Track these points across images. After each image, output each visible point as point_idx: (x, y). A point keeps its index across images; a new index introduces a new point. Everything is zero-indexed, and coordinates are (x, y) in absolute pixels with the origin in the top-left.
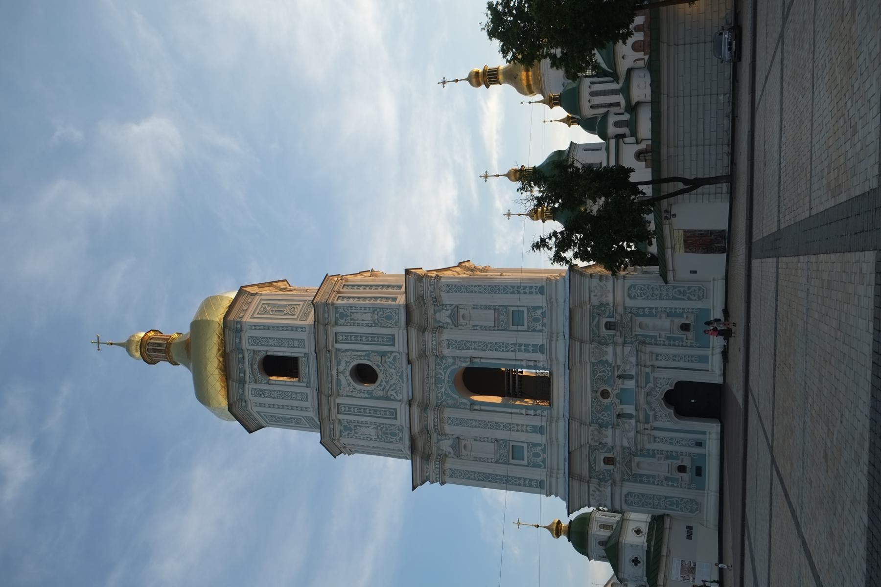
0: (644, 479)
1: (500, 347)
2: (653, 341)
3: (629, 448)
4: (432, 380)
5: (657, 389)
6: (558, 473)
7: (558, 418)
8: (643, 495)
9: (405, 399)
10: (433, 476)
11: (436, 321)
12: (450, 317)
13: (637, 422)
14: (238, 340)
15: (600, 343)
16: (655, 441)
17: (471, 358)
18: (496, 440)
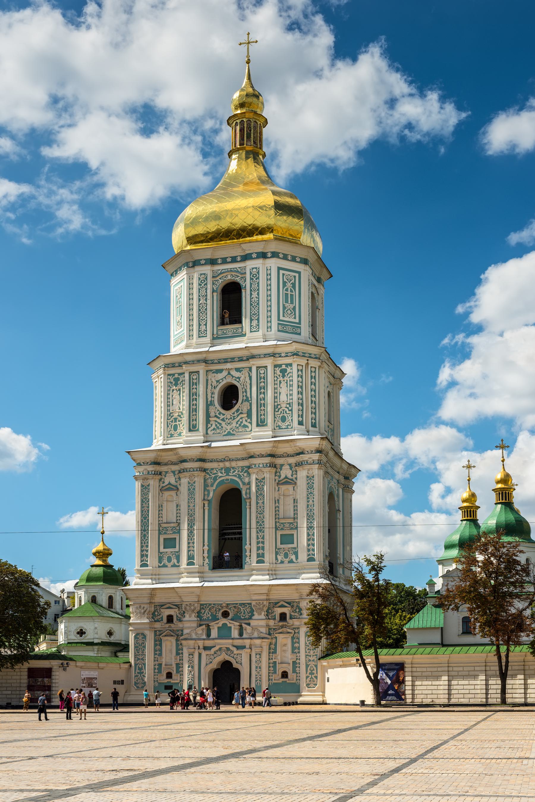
0: (158, 647)
1: (261, 525)
2: (272, 651)
3: (182, 635)
4: (227, 464)
5: (232, 655)
8: (144, 647)
9: (209, 439)
10: (141, 469)
11: (282, 465)
12: (286, 477)
13: (204, 639)
15: (269, 608)
16: (189, 655)
17: (250, 498)
18: (179, 524)
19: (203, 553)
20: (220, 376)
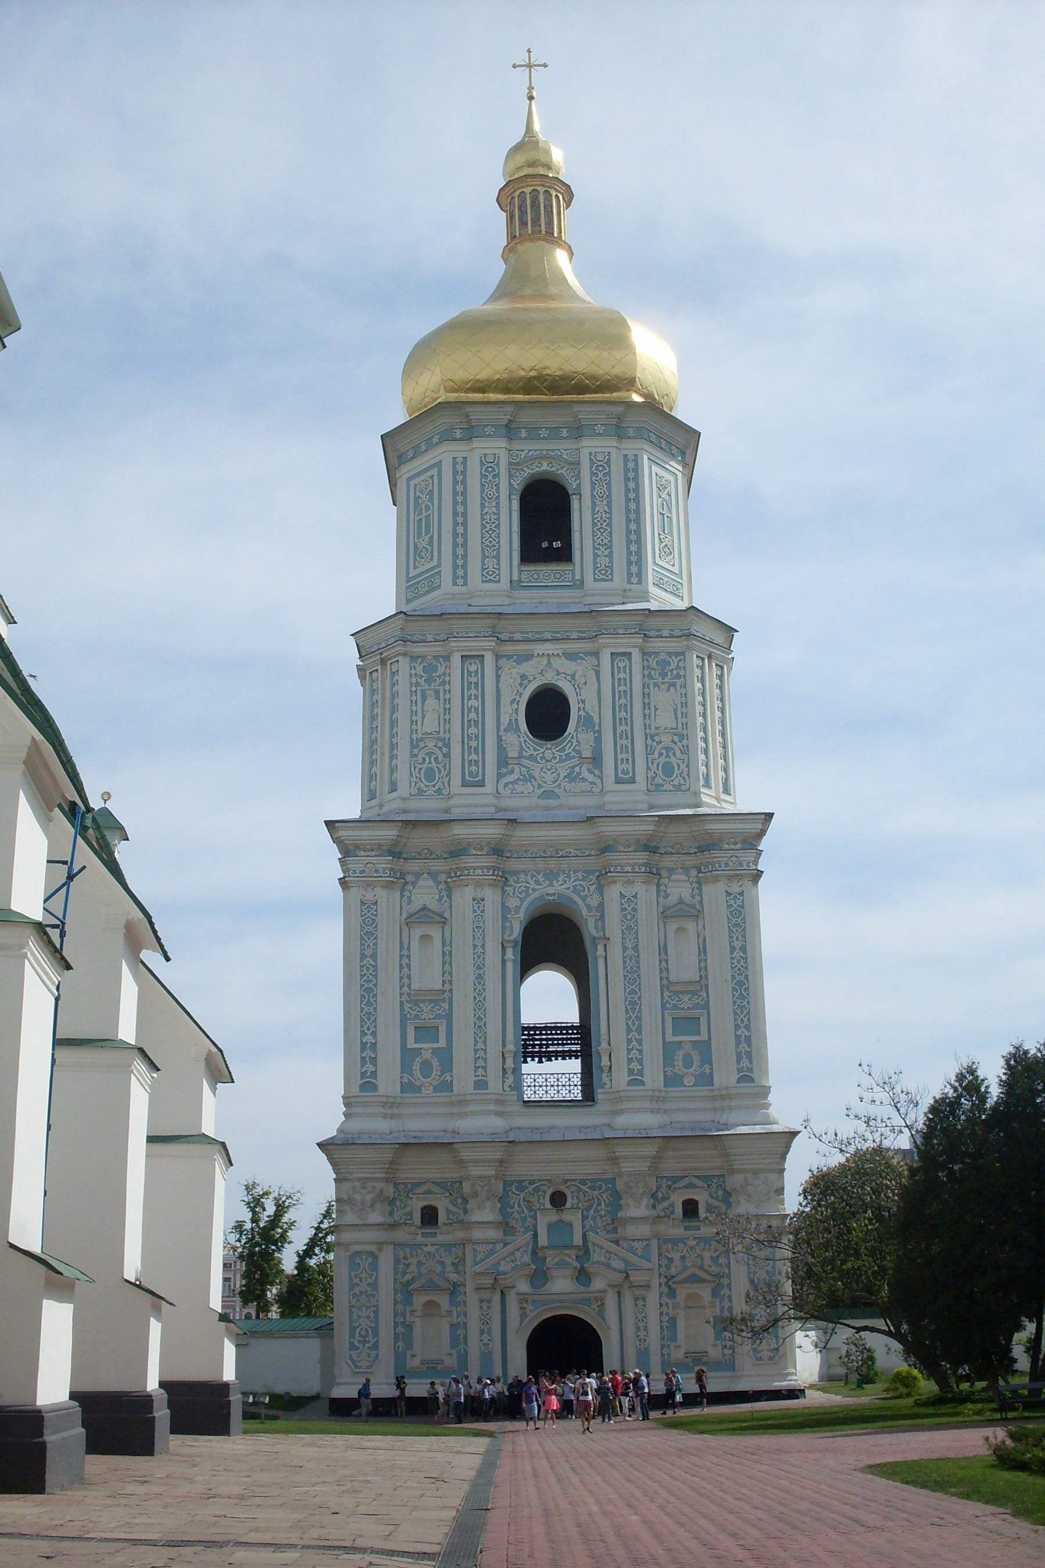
6: (392, 1117)
7: (499, 1114)
9: (506, 803)
10: (356, 864)
14: (599, 429)
19: (504, 1062)
20: (529, 668)
